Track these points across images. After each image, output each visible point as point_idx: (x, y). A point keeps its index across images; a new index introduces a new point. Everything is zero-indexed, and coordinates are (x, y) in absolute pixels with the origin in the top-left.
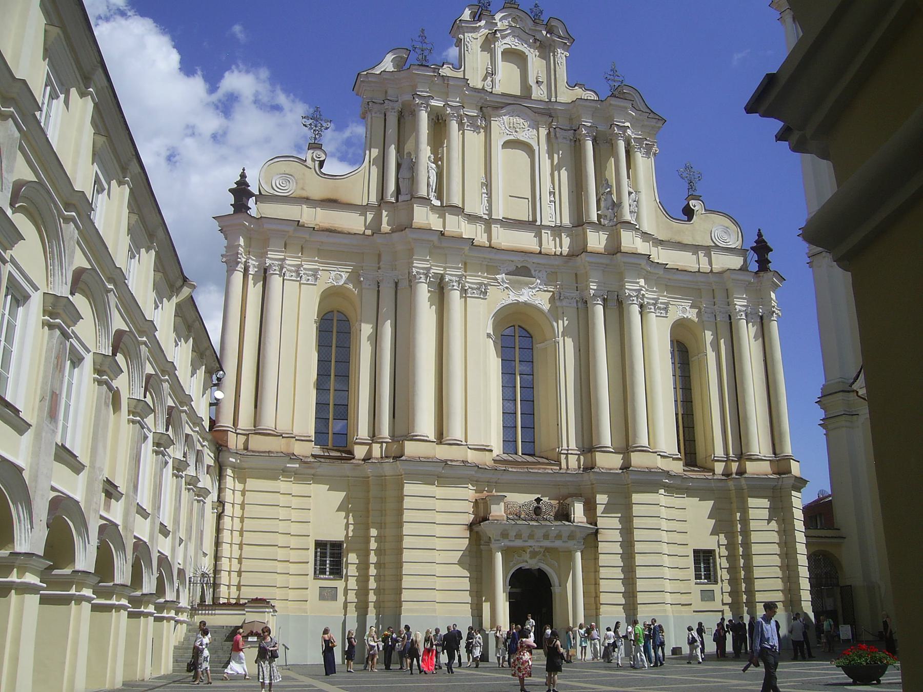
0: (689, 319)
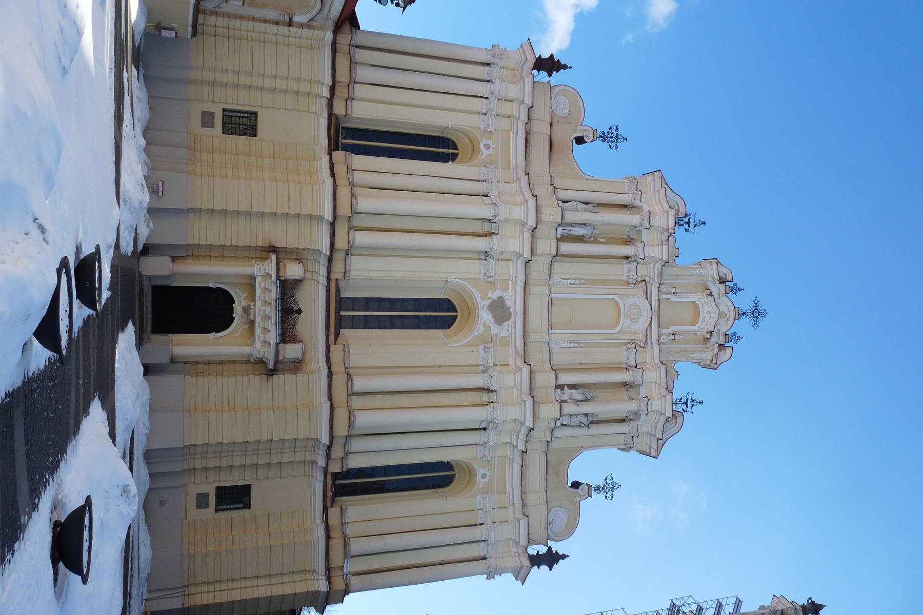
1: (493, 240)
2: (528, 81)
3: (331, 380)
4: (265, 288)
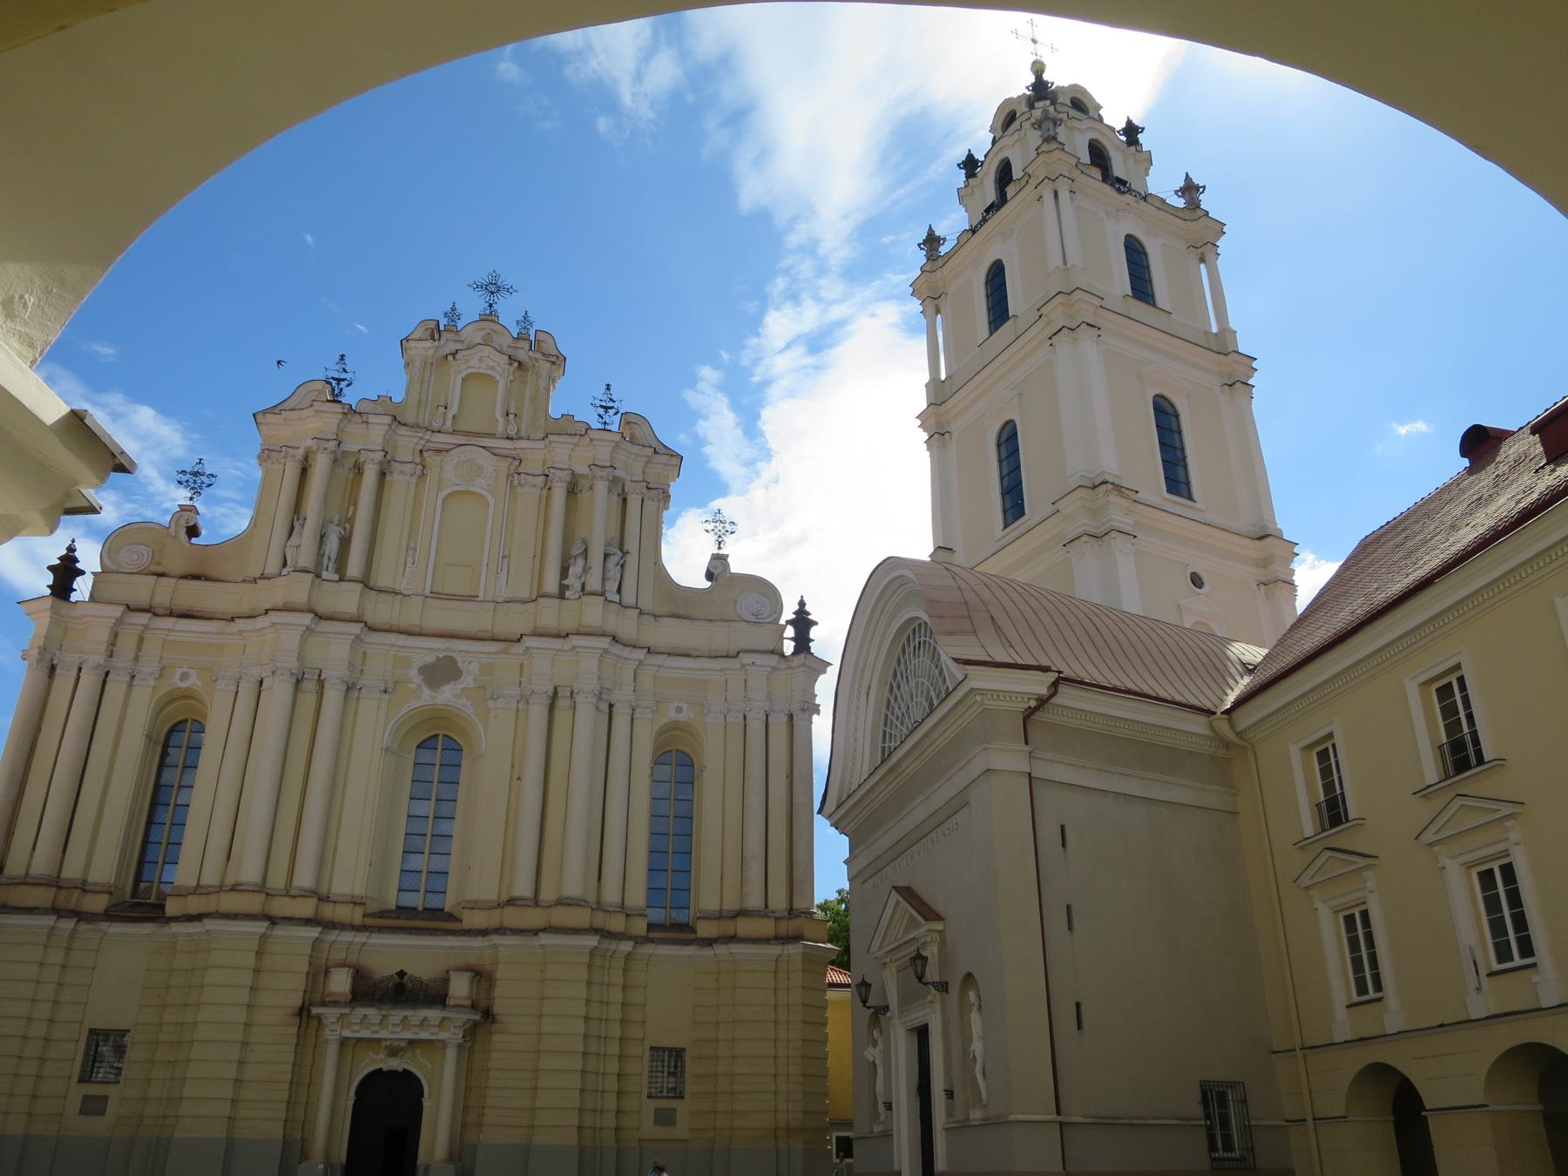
1: (328, 679)
3: (511, 930)
4: (361, 1023)
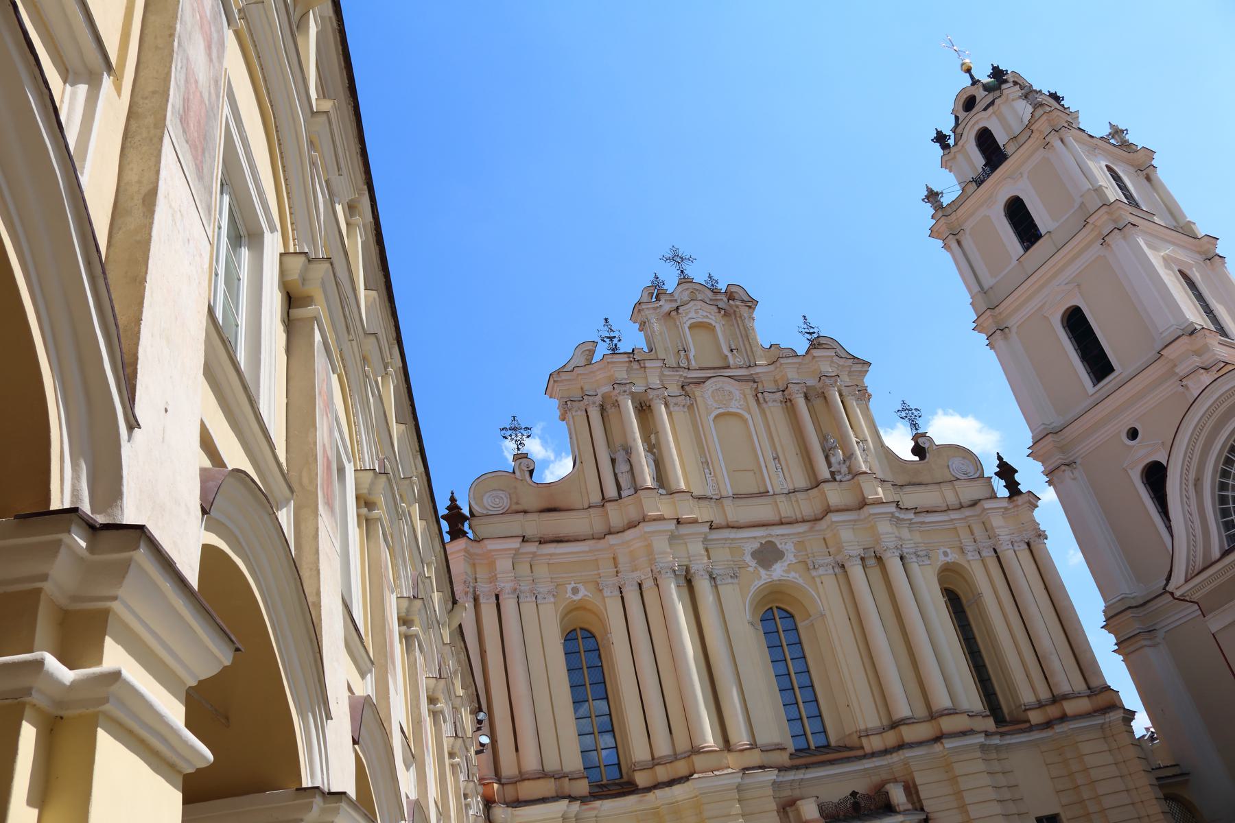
0: (953, 562)
2: (490, 545)
3: (912, 743)
